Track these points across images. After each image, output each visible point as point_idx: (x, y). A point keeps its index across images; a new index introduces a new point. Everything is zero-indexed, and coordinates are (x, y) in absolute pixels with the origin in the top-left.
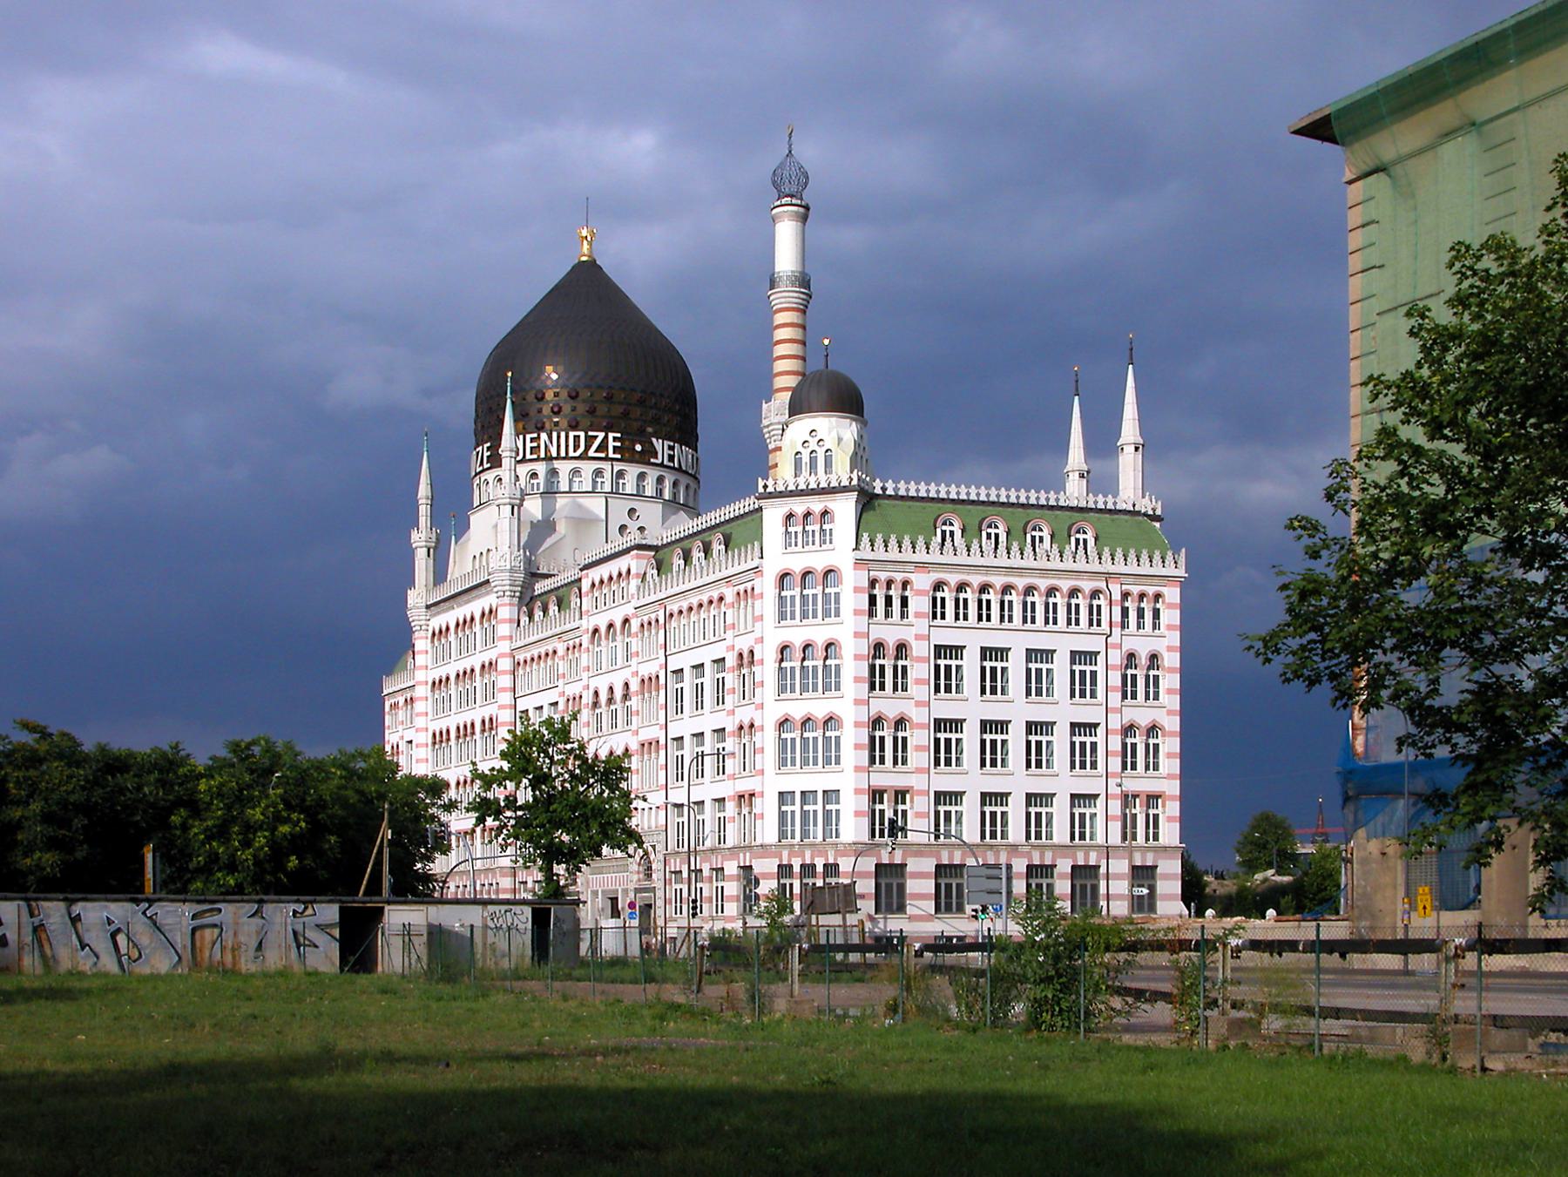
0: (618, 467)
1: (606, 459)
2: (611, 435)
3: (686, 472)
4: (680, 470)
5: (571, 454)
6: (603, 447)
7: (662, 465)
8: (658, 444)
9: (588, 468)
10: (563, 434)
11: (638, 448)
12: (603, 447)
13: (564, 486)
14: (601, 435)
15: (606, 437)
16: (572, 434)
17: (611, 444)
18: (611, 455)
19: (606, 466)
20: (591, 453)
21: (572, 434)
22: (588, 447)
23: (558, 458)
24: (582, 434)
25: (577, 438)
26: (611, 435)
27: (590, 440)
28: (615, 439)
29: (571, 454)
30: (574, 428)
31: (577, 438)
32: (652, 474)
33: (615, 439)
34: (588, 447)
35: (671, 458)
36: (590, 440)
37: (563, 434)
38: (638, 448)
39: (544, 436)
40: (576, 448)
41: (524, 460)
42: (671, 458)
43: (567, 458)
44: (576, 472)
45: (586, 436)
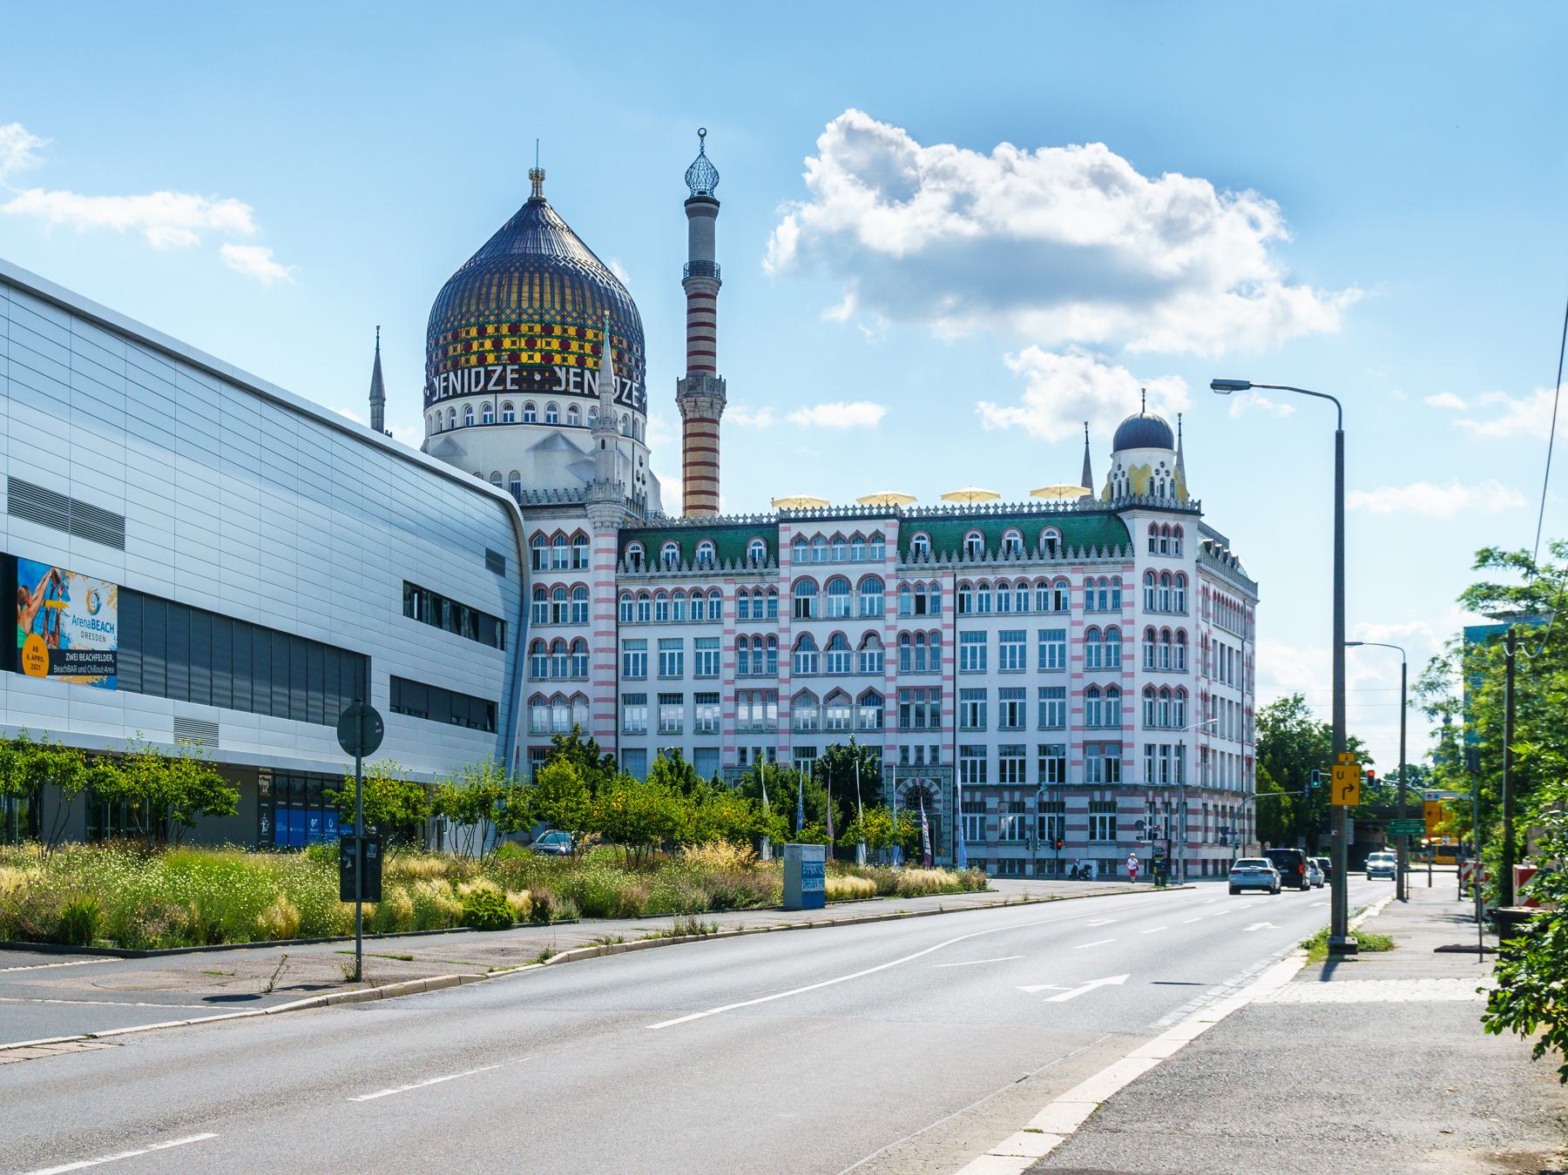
1: (505, 391)
5: (473, 389)
6: (501, 380)
7: (566, 392)
8: (561, 374)
12: (501, 380)
14: (499, 369)
15: (504, 370)
17: (509, 376)
18: (509, 387)
20: (490, 387)
23: (463, 395)
25: (478, 373)
26: (509, 368)
27: (489, 375)
31: (478, 373)
35: (579, 385)
36: (489, 375)
39: (452, 375)
41: (440, 400)
42: (577, 385)
43: (470, 393)
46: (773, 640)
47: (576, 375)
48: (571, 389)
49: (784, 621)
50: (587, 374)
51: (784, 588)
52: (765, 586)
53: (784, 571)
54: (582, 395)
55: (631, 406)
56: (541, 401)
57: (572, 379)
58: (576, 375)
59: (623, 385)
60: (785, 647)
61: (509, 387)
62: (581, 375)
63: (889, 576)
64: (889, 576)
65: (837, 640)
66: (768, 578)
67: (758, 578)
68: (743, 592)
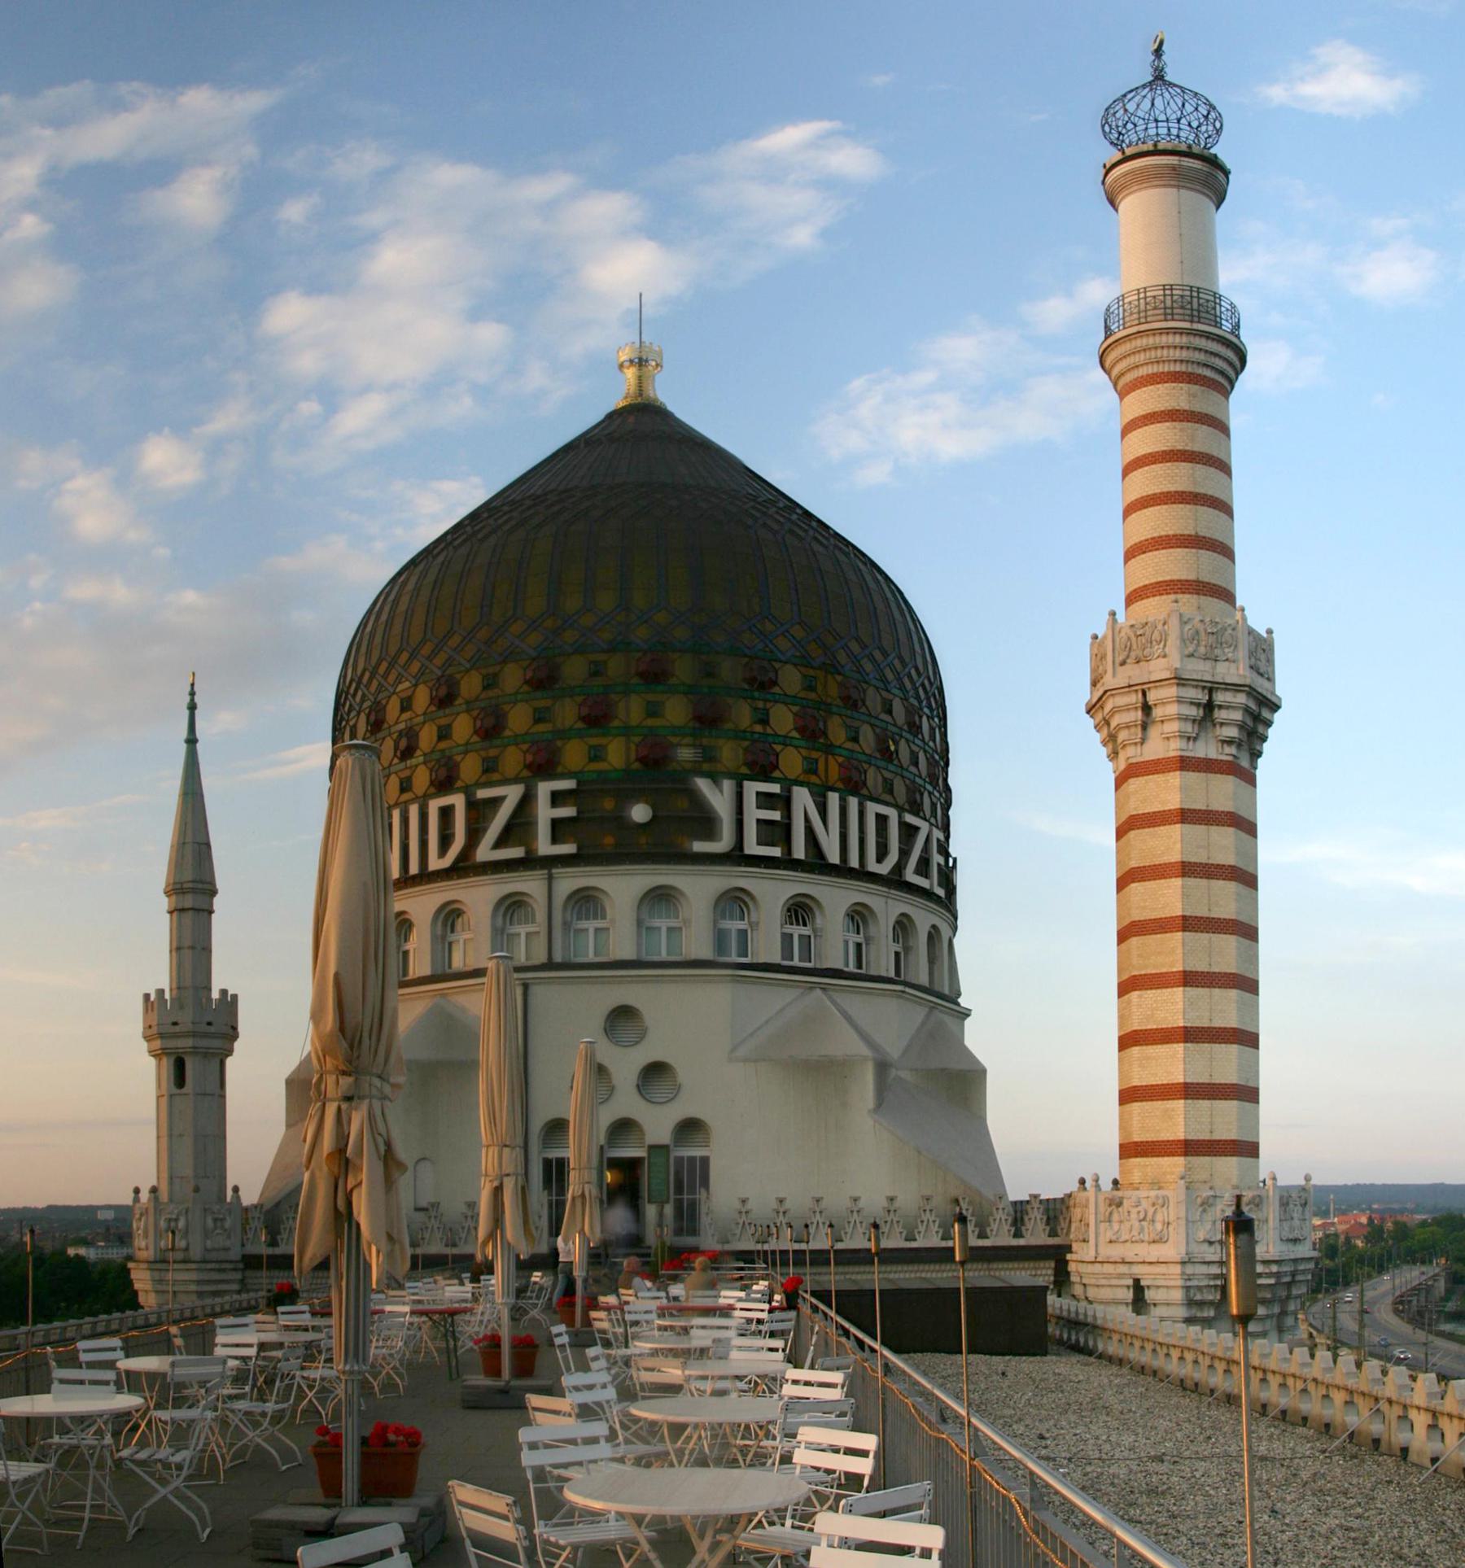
0: (569, 881)
2: (544, 789)
3: (842, 871)
4: (817, 863)
6: (518, 827)
7: (737, 857)
8: (719, 798)
9: (479, 898)
10: (414, 810)
11: (640, 813)
12: (518, 827)
13: (420, 966)
14: (512, 794)
15: (526, 802)
16: (434, 806)
17: (545, 813)
18: (545, 846)
19: (530, 884)
20: (484, 852)
21: (434, 806)
22: (474, 835)
24: (458, 801)
25: (446, 813)
27: (480, 812)
28: (557, 798)
29: (435, 863)
30: (444, 785)
31: (446, 813)
32: (699, 888)
33: (557, 798)
34: (474, 835)
35: (776, 832)
36: (480, 812)
37: (414, 810)
38: (640, 813)
40: (445, 841)
42: (776, 832)
43: (426, 877)
44: (450, 916)
45: (472, 805)
47: (765, 800)
48: (752, 848)
50: (802, 798)
54: (788, 863)
57: (753, 814)
58: (765, 800)
59: (909, 832)
62: (784, 802)
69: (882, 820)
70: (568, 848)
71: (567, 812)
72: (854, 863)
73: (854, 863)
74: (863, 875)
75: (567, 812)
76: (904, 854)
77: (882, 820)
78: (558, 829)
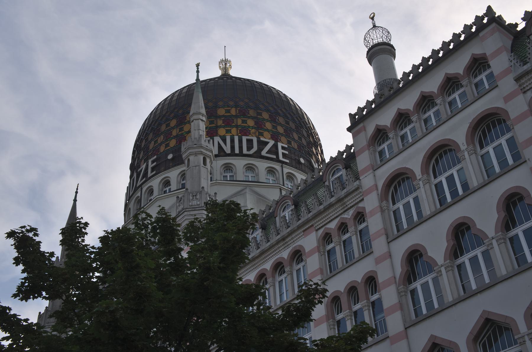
15: (147, 165)
17: (150, 166)
46: (371, 281)
49: (379, 246)
51: (371, 203)
52: (349, 215)
53: (367, 181)
55: (277, 160)
56: (173, 175)
60: (387, 283)
61: (150, 174)
63: (508, 99)
64: (508, 99)
65: (462, 234)
66: (349, 202)
67: (338, 209)
68: (327, 238)
69: (250, 142)
70: (154, 172)
71: (155, 164)
72: (237, 151)
73: (237, 151)
74: (241, 154)
75: (155, 164)
76: (260, 150)
77: (250, 142)
78: (153, 169)
